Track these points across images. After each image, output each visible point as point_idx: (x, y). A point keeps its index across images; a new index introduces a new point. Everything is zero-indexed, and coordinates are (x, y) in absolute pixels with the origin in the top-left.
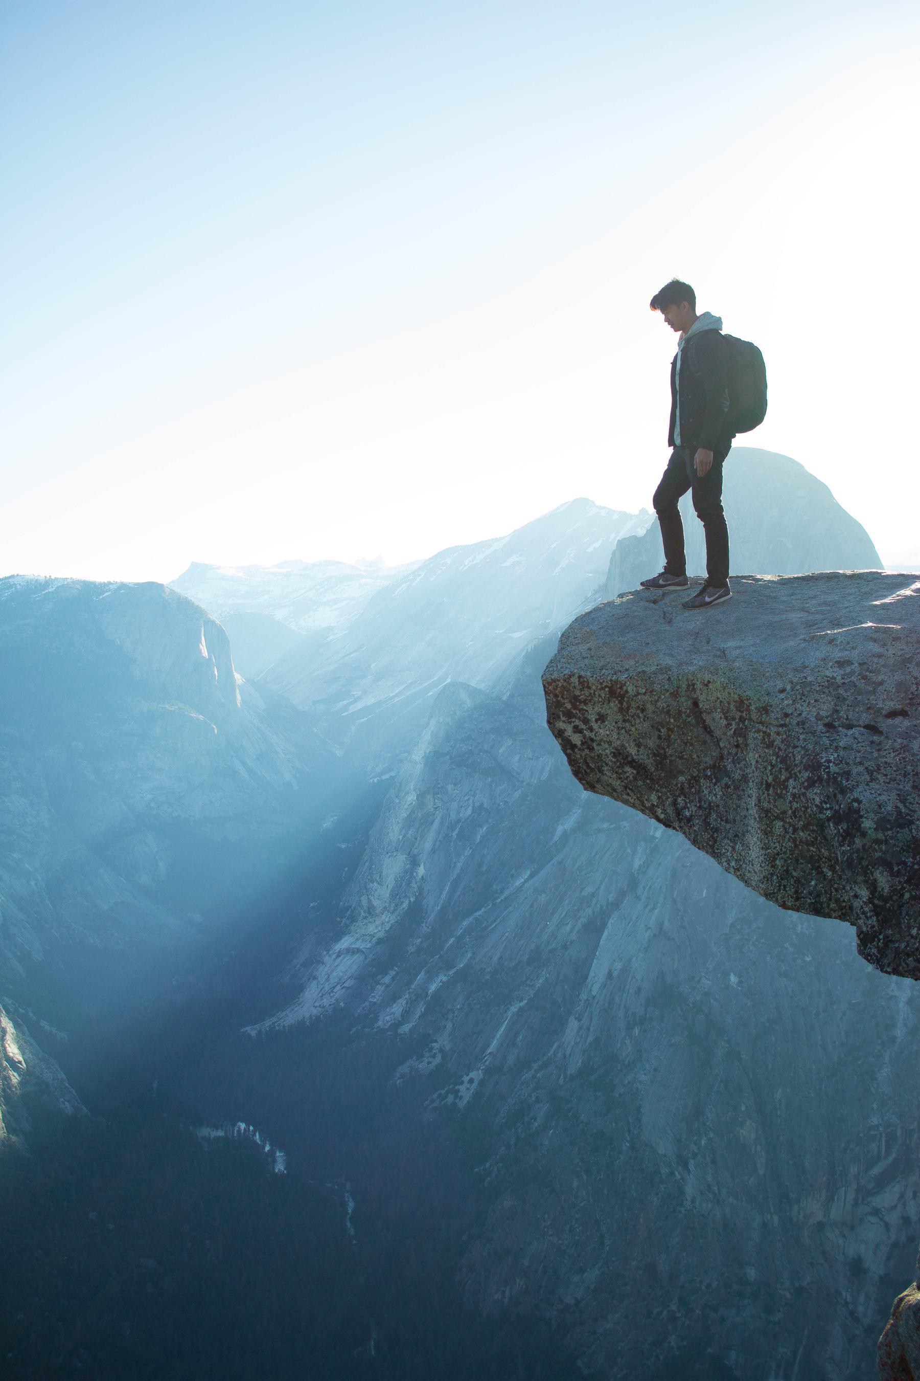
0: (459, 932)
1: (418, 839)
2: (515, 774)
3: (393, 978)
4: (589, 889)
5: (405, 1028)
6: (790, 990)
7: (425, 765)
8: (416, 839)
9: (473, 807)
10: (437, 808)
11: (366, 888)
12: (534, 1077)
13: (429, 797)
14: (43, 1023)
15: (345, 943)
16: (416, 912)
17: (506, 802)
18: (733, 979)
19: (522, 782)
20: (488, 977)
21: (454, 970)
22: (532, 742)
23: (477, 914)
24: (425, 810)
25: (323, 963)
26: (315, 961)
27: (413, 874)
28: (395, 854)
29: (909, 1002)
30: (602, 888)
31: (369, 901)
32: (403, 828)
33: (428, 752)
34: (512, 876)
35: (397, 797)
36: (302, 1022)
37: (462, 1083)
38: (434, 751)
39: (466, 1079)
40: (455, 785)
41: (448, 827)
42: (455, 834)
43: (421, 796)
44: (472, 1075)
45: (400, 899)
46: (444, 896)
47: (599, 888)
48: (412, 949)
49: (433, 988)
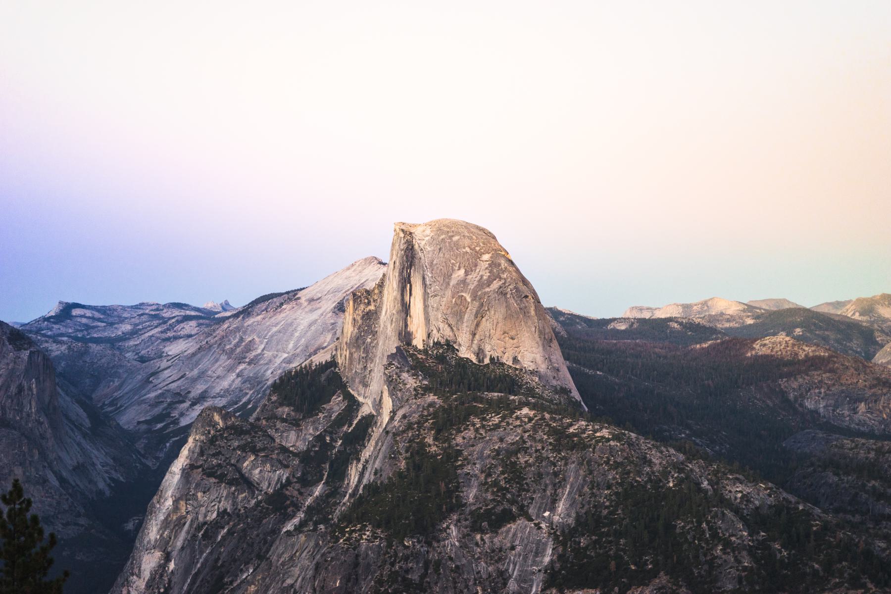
1: (173, 538)
2: (256, 485)
4: (289, 581)
7: (181, 477)
8: (170, 538)
9: (218, 511)
10: (188, 512)
11: (127, 580)
13: (182, 503)
17: (246, 507)
19: (261, 491)
22: (272, 458)
24: (179, 514)
27: (165, 568)
28: (153, 551)
30: (300, 579)
32: (161, 529)
33: (185, 465)
34: (241, 570)
35: (158, 502)
38: (190, 464)
40: (204, 493)
41: (196, 529)
42: (200, 535)
43: (176, 502)
45: (153, 589)
46: (185, 588)
47: (296, 581)
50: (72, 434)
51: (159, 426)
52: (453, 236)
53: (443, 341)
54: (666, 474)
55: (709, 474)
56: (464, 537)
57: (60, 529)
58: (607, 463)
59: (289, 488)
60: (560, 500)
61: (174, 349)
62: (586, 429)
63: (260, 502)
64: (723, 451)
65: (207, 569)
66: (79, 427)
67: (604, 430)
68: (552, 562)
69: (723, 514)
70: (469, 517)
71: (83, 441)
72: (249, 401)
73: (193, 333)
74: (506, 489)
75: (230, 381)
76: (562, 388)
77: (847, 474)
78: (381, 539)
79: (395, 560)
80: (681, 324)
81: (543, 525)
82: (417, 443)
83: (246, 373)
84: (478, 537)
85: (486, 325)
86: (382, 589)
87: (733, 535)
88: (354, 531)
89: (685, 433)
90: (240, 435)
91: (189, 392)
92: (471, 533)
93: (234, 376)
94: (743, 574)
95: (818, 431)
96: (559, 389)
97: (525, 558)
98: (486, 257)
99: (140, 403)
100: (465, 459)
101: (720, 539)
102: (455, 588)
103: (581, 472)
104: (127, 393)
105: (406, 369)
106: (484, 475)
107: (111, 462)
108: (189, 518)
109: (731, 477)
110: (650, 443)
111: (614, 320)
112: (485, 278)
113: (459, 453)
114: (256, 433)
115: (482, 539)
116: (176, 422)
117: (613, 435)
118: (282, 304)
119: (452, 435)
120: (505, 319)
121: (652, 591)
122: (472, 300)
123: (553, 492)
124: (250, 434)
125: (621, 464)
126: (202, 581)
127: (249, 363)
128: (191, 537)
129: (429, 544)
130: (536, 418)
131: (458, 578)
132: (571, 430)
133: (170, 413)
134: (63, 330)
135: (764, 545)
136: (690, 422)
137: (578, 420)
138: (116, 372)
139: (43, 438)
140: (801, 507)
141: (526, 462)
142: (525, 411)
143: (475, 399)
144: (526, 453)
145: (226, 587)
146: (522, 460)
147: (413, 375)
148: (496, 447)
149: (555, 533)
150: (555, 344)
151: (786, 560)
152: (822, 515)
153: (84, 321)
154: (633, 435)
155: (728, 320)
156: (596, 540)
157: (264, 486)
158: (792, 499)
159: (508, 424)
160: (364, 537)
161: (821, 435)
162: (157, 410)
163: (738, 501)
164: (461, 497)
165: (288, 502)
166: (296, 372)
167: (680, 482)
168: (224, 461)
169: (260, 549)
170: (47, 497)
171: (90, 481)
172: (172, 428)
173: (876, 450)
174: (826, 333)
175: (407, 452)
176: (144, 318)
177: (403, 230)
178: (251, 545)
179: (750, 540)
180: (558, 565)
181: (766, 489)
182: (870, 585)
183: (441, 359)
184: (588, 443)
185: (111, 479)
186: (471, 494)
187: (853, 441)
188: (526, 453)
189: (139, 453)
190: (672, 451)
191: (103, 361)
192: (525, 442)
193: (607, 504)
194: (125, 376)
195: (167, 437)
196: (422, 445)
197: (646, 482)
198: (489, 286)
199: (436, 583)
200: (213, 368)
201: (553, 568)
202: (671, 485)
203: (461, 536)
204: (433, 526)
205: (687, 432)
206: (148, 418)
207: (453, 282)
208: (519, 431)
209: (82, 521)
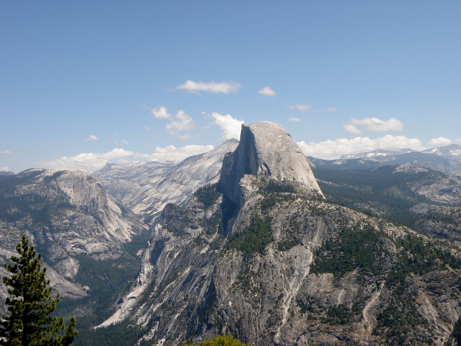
0: (165, 290)
3: (144, 307)
4: (204, 274)
6: (249, 307)
7: (159, 232)
12: (179, 340)
15: (131, 295)
16: (153, 284)
18: (230, 303)
20: (171, 305)
21: (162, 303)
25: (123, 302)
26: (121, 301)
29: (289, 310)
31: (140, 279)
34: (185, 270)
37: (158, 343)
39: (159, 342)
42: (168, 256)
44: (161, 340)
46: (162, 277)
47: (207, 273)
48: (151, 296)
49: (154, 310)
50: (114, 217)
51: (149, 212)
52: (266, 128)
53: (264, 173)
54: (359, 224)
55: (378, 223)
56: (275, 253)
57: (111, 255)
58: (334, 220)
59: (203, 235)
60: (315, 236)
61: (154, 181)
62: (324, 207)
63: (191, 242)
64: (384, 213)
65: (171, 270)
67: (333, 206)
68: (313, 262)
69: (385, 240)
70: (277, 245)
71: (119, 219)
72: (185, 201)
73: (161, 173)
74: (292, 233)
75: (178, 192)
76: (314, 190)
77: (438, 222)
78: (241, 254)
79: (247, 264)
80: (364, 161)
81: (308, 247)
82: (254, 215)
83: (183, 189)
84: (281, 253)
85: (281, 165)
86: (242, 276)
87: (389, 249)
88: (230, 252)
89: (367, 207)
90: (182, 214)
91: (161, 198)
92: (278, 251)
93: (178, 190)
94: (394, 265)
95: (425, 204)
96: (313, 190)
97: (301, 261)
98: (280, 136)
99: (141, 203)
100: (275, 221)
101: (384, 251)
102: (273, 274)
103: (324, 224)
104: (136, 199)
105: (249, 184)
106: (282, 227)
107: (131, 227)
109: (388, 224)
110: (352, 211)
111: (335, 160)
112: (280, 145)
113: (272, 218)
114: (188, 213)
115: (283, 254)
117: (337, 208)
118: (197, 160)
119: (268, 211)
120: (289, 162)
121: (356, 273)
122: (275, 155)
123: (312, 233)
124: (186, 214)
125: (340, 220)
126: (169, 275)
127: (185, 185)
128: (164, 257)
129: (261, 257)
130: (304, 203)
131: (274, 270)
132: (319, 207)
133: (153, 207)
134: (108, 174)
135: (402, 253)
136: (369, 202)
137: (321, 203)
138: (131, 191)
139: (102, 219)
140: (418, 236)
141: (300, 221)
142: (299, 200)
143: (278, 195)
144: (300, 217)
145: (179, 277)
146: (299, 221)
147: (252, 187)
148: (288, 215)
149: (313, 250)
150: (311, 172)
151: (413, 259)
152: (428, 239)
153: (117, 170)
154: (344, 208)
155: (385, 159)
156: (331, 253)
157: (193, 235)
158: (414, 232)
159: (292, 205)
160: (234, 254)
161: (426, 206)
162: (149, 206)
163: (391, 234)
164: (273, 236)
165: (203, 241)
166: (204, 187)
167: (366, 227)
168: (176, 225)
169: (192, 261)
170: (105, 243)
172: (155, 213)
173: (451, 211)
174: (428, 162)
175: (250, 219)
176: (142, 168)
177: (245, 127)
178: (188, 260)
179: (396, 251)
180: (315, 264)
181: (403, 229)
182: (450, 268)
183: (263, 180)
184: (326, 212)
186: (278, 235)
187: (440, 208)
188: (300, 217)
189: (141, 223)
190: (362, 214)
191: (125, 186)
192: (299, 213)
193: (335, 237)
195: (153, 216)
196: (257, 215)
197: (351, 228)
198: (282, 148)
199: (264, 273)
200: (170, 188)
201: (313, 265)
202: (362, 228)
203: (274, 252)
204: (263, 249)
205: (368, 206)
206: (145, 209)
207: (266, 148)
208: (297, 208)
209: (120, 251)
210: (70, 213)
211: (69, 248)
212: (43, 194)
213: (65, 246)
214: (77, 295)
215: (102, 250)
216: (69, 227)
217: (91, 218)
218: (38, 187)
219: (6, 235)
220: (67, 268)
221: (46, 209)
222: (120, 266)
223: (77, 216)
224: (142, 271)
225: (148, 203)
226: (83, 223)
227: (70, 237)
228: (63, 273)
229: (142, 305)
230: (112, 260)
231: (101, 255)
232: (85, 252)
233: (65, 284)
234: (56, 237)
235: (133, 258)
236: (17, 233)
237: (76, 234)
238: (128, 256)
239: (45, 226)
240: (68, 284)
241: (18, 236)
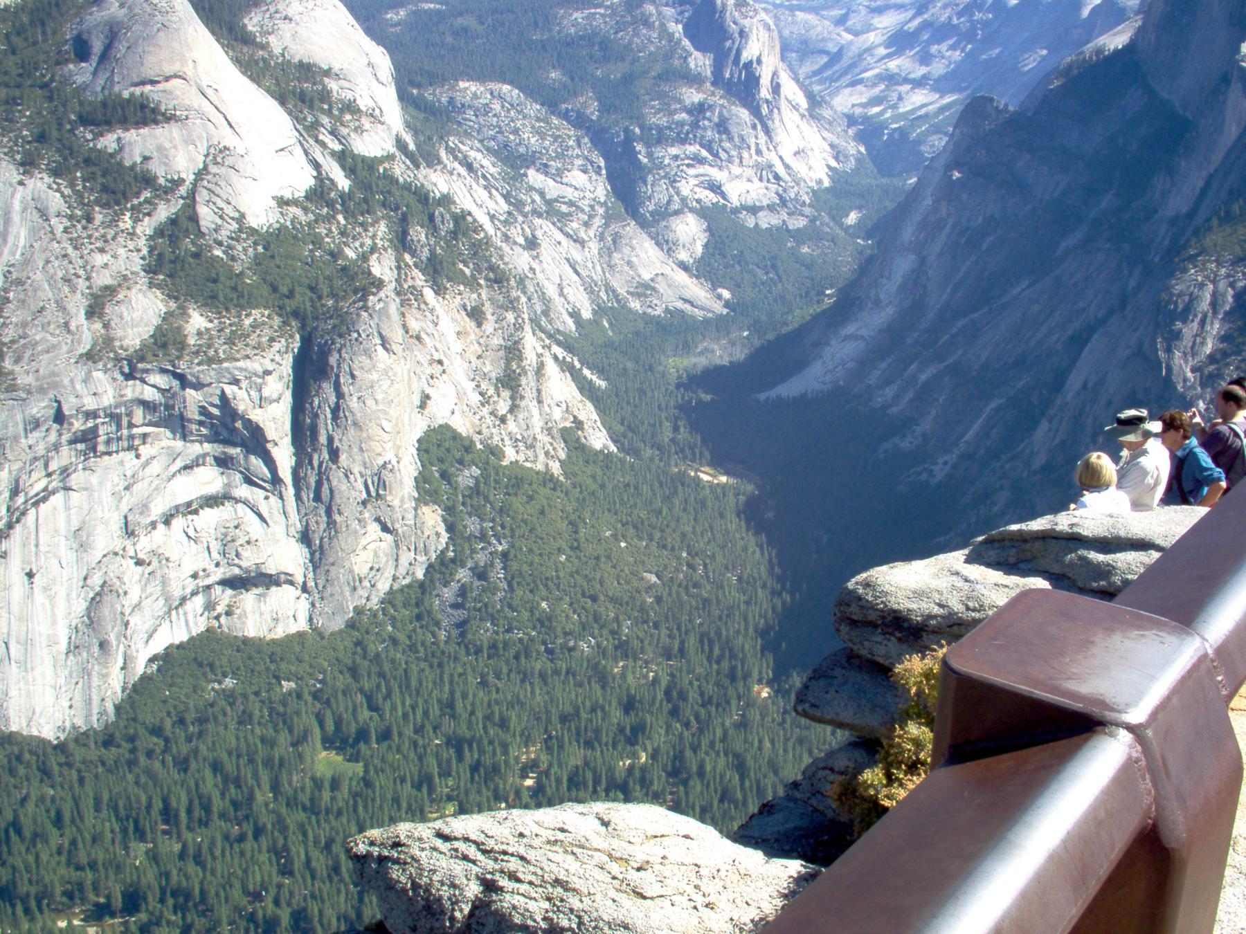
0: (955, 330)
5: (894, 410)
14: (586, 372)
15: (850, 329)
23: (974, 316)
36: (803, 396)
42: (964, 240)
48: (909, 341)
49: (923, 377)
51: (876, 110)
66: (796, 108)
107: (828, 149)
108: (951, 221)
116: (894, 107)
162: (876, 91)
171: (810, 168)
185: (828, 167)
194: (835, 50)
206: (864, 100)
209: (807, 210)
210: (693, 96)
211: (686, 188)
212: (624, 37)
213: (675, 181)
214: (702, 309)
215: (765, 204)
216: (688, 133)
217: (744, 114)
218: (609, 16)
219: (543, 139)
220: (681, 242)
221: (628, 79)
222: (805, 250)
223: (710, 106)
224: (886, 273)
225: (875, 85)
226: (722, 126)
227: (689, 158)
228: (669, 250)
229: (883, 359)
230: (788, 231)
231: (761, 214)
232: (722, 201)
233: (675, 277)
234: (656, 155)
235: (838, 231)
236: (569, 137)
237: (704, 153)
238: (827, 225)
239: (631, 124)
240: (682, 277)
241: (571, 143)
